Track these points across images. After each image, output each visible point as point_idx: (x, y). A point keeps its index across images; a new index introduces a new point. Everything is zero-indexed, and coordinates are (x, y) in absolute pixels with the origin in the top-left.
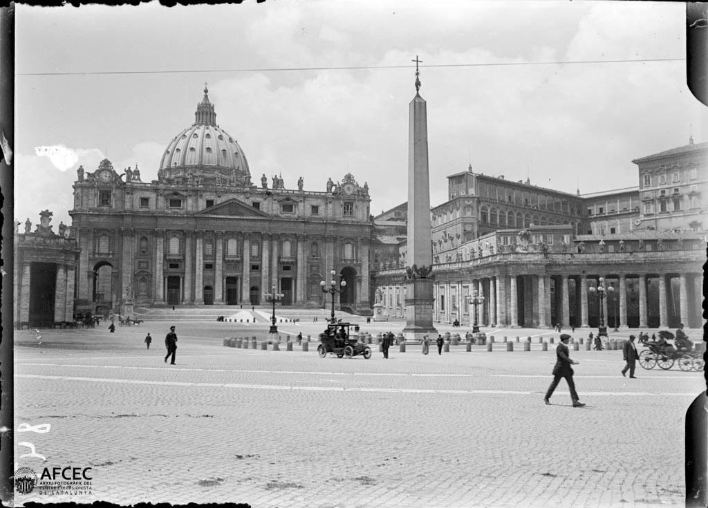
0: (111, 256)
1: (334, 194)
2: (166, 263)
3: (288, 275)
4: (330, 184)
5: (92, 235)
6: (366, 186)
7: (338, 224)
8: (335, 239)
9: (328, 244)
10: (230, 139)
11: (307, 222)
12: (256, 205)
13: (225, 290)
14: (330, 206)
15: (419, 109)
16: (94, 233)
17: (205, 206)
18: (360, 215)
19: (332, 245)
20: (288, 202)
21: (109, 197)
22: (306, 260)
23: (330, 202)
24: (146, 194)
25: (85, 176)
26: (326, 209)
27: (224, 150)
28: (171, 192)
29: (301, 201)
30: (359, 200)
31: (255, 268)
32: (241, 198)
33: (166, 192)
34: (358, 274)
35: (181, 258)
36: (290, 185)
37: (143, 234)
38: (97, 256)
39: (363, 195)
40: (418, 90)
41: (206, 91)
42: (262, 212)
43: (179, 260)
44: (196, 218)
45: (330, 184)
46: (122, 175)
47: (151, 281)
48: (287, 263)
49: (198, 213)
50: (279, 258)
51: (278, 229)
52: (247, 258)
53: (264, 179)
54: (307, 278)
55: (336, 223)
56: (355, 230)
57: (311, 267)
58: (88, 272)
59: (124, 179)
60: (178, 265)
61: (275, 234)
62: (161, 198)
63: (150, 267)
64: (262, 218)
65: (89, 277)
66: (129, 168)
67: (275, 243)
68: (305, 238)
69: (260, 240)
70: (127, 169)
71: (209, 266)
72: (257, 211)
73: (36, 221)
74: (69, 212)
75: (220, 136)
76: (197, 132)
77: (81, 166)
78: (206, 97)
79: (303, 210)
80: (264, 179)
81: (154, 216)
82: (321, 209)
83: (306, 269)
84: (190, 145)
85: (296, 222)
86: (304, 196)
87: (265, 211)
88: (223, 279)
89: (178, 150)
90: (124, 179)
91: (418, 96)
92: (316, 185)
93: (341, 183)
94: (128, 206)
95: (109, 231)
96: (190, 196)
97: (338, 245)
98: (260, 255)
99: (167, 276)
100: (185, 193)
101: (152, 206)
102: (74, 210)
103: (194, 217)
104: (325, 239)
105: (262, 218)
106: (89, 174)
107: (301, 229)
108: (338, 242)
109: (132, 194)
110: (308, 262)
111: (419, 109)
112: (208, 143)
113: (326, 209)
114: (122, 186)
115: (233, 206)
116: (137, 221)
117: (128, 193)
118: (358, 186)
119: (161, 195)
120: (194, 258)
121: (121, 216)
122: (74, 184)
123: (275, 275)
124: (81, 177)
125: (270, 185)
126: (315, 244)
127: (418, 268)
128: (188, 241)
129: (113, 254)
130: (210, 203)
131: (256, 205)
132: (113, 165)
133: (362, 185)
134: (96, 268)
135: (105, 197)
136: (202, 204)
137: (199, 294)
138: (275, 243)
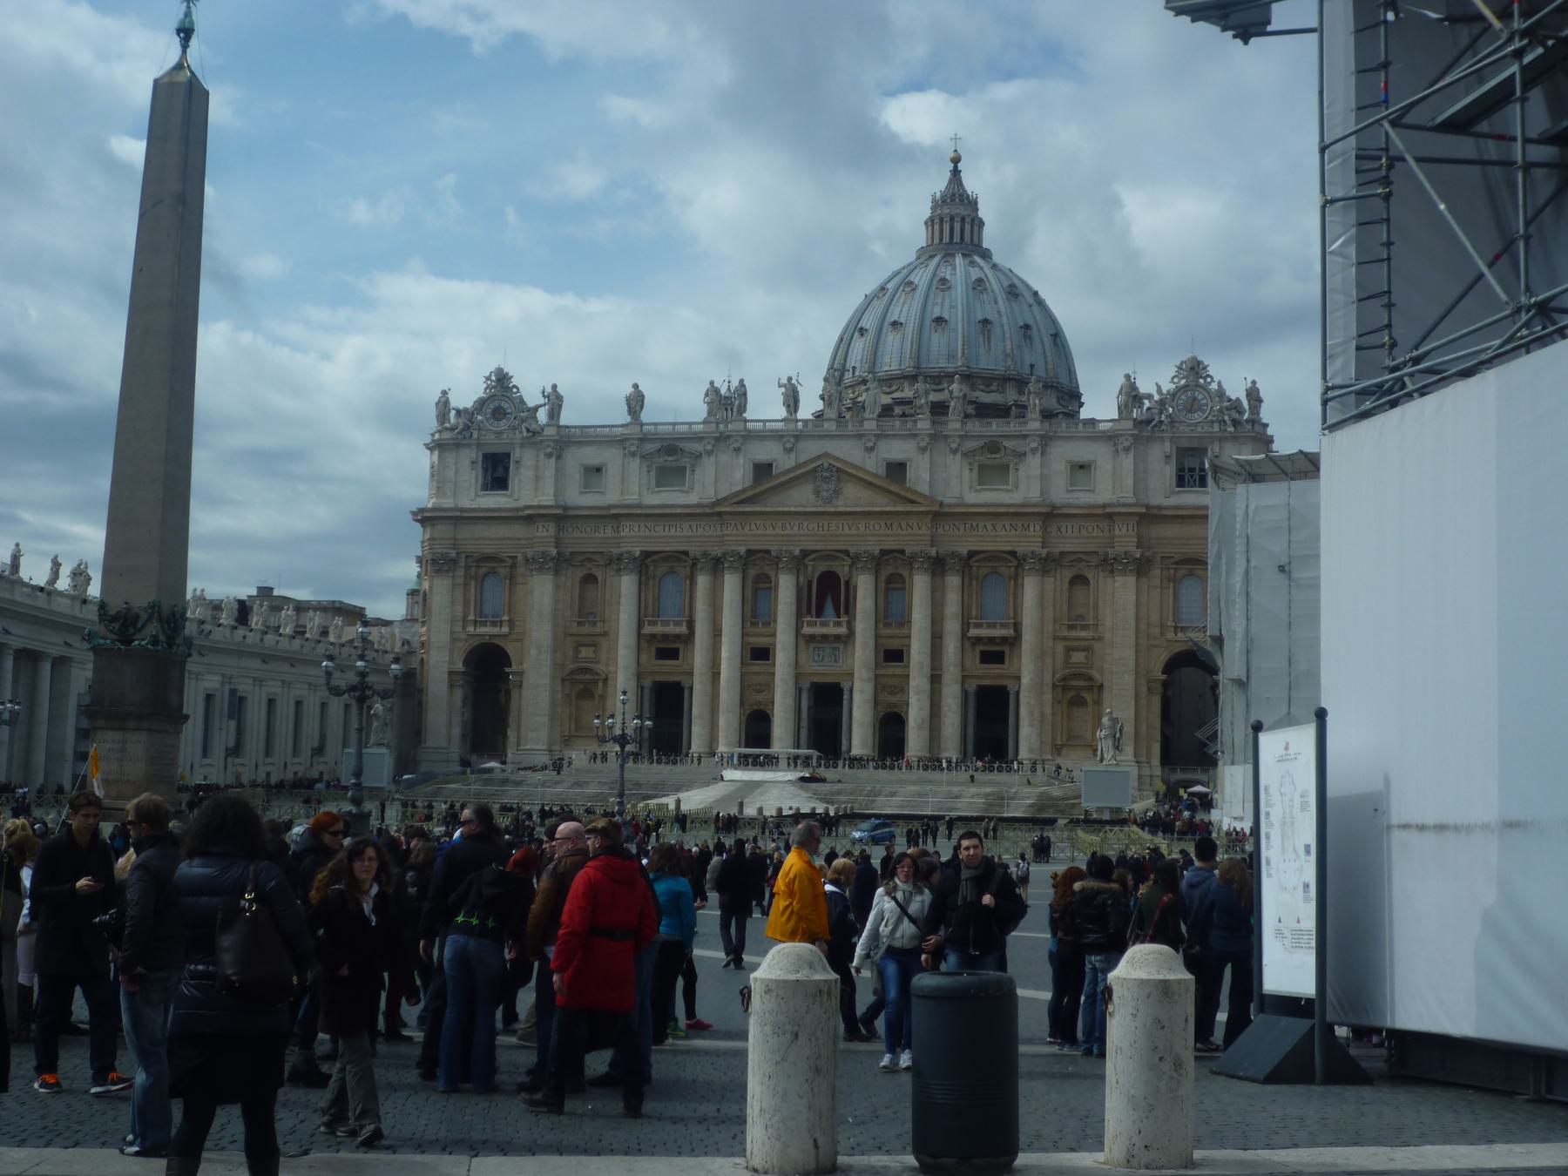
0: (505, 629)
1: (1138, 423)
2: (644, 644)
3: (991, 675)
5: (461, 572)
6: (1254, 395)
7: (1149, 516)
8: (1141, 567)
9: (1120, 580)
10: (1012, 286)
11: (1051, 516)
12: (897, 469)
13: (804, 723)
14: (1127, 462)
16: (467, 567)
17: (749, 482)
19: (1131, 580)
21: (507, 470)
22: (1049, 628)
23: (1127, 450)
24: (592, 456)
27: (986, 322)
28: (657, 445)
29: (1034, 451)
30: (1221, 439)
31: (895, 655)
33: (649, 447)
35: (683, 629)
37: (589, 565)
38: (471, 629)
40: (185, 46)
41: (956, 161)
42: (915, 492)
43: (678, 637)
44: (720, 514)
46: (536, 408)
47: (603, 697)
48: (992, 640)
49: (719, 502)
50: (965, 626)
51: (963, 541)
54: (1054, 686)
55: (1142, 516)
57: (1069, 650)
58: (451, 673)
59: (542, 416)
60: (677, 650)
61: (954, 555)
62: (635, 464)
64: (909, 508)
65: (451, 686)
66: (554, 387)
67: (953, 581)
68: (1048, 564)
70: (549, 390)
72: (894, 488)
74: (414, 514)
75: (980, 281)
76: (946, 272)
77: (444, 393)
78: (956, 173)
81: (615, 517)
83: (1049, 660)
84: (894, 316)
85: (1017, 515)
87: (924, 489)
88: (799, 690)
89: (862, 331)
90: (542, 416)
93: (1167, 387)
94: (546, 498)
95: (500, 560)
96: (709, 453)
97: (1157, 582)
98: (905, 622)
99: (647, 683)
100: (697, 447)
101: (611, 495)
102: (421, 510)
103: (711, 513)
104: (1109, 564)
105: (909, 508)
106: (459, 412)
107: (1028, 540)
108: (1156, 572)
109: (559, 457)
110: (1055, 638)
114: (534, 436)
117: (549, 456)
118: (1221, 393)
119: (633, 454)
120: (716, 633)
121: (530, 517)
122: (429, 440)
127: (112, 612)
128: (703, 581)
129: (511, 623)
130: (762, 470)
131: (897, 469)
132: (515, 381)
133: (1236, 391)
135: (496, 472)
136: (738, 476)
138: (953, 581)
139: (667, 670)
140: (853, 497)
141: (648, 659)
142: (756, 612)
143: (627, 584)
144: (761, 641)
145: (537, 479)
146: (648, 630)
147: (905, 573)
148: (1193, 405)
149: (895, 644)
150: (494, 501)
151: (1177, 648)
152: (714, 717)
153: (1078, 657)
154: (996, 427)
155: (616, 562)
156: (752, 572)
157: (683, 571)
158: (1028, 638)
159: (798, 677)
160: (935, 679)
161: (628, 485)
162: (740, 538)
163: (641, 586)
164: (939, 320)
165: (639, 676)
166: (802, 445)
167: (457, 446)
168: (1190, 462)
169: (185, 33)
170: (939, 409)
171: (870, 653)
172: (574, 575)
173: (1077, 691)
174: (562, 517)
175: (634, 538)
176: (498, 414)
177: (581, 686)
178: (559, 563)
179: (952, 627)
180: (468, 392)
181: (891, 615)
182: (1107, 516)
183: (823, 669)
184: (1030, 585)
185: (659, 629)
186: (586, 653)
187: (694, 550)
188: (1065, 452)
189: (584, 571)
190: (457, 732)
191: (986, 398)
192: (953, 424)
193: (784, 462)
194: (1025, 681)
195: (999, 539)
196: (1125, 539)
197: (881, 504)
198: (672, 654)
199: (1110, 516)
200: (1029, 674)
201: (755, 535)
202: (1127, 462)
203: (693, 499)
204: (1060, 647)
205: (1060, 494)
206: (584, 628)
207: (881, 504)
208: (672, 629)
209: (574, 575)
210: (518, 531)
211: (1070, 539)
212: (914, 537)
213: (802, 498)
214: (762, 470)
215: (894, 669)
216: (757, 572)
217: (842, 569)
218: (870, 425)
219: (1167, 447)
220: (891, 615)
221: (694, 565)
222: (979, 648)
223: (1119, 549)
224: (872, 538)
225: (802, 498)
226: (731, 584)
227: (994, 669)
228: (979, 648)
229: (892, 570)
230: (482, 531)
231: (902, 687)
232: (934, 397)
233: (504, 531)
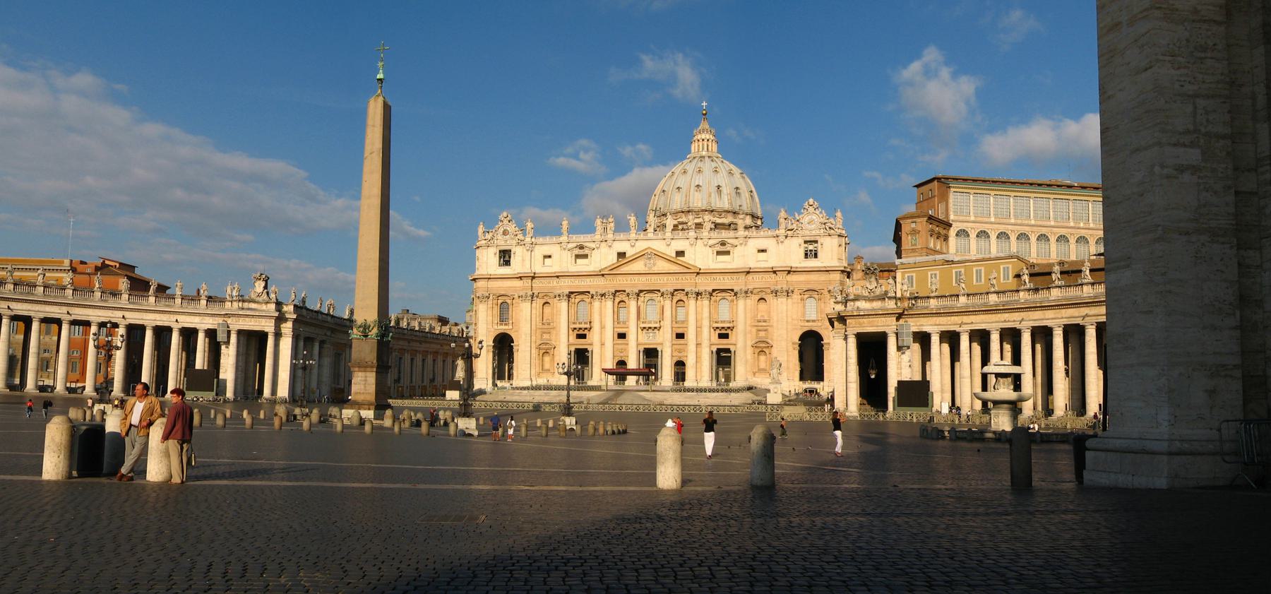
8: (788, 293)
22: (749, 322)
32: (659, 246)
34: (825, 341)
52: (667, 324)
56: (823, 277)
63: (553, 337)
69: (685, 298)
98: (685, 321)
99: (573, 349)
100: (593, 245)
101: (553, 267)
107: (738, 283)
108: (796, 296)
112: (698, 180)
116: (537, 283)
120: (602, 327)
123: (705, 343)
128: (596, 304)
130: (621, 255)
131: (680, 254)
136: (613, 259)
139: (581, 344)
140: (662, 266)
141: (573, 338)
143: (564, 305)
146: (573, 326)
147: (685, 298)
149: (680, 331)
150: (505, 271)
151: (806, 329)
153: (762, 334)
154: (724, 234)
156: (617, 300)
157: (587, 298)
158: (740, 327)
159: (638, 345)
160: (698, 345)
164: (698, 186)
166: (638, 244)
168: (811, 247)
170: (699, 226)
172: (538, 303)
173: (762, 347)
175: (566, 285)
177: (545, 350)
179: (706, 323)
183: (649, 340)
185: (577, 326)
186: (546, 336)
187: (592, 292)
190: (490, 371)
191: (719, 221)
192: (705, 233)
193: (630, 252)
194: (740, 345)
195: (726, 282)
196: (782, 281)
198: (584, 336)
199: (775, 272)
200: (741, 345)
201: (620, 282)
204: (754, 330)
205: (752, 264)
206: (546, 326)
208: (583, 326)
209: (538, 303)
211: (755, 282)
212: (688, 283)
213: (638, 266)
214: (621, 255)
215: (681, 341)
218: (668, 235)
219: (801, 241)
222: (718, 331)
223: (778, 288)
224: (668, 284)
225: (638, 266)
226: (609, 304)
227: (724, 341)
228: (718, 331)
232: (697, 221)
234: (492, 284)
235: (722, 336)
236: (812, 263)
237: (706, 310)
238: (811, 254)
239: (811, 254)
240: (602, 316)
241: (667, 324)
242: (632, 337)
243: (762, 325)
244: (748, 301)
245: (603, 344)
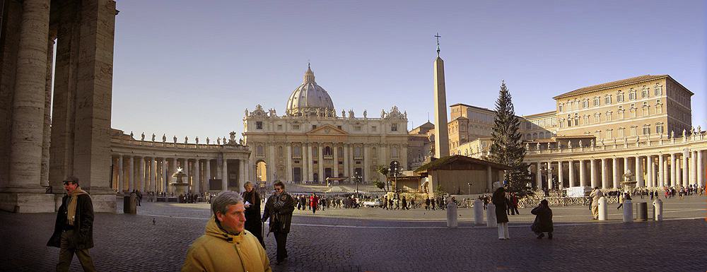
4: (384, 113)
6: (405, 113)
8: (386, 146)
9: (382, 148)
15: (440, 63)
18: (400, 132)
20: (358, 124)
21: (261, 124)
25: (249, 115)
26: (381, 129)
31: (340, 163)
36: (359, 115)
39: (403, 119)
45: (384, 113)
50: (354, 157)
52: (336, 157)
53: (344, 112)
56: (399, 139)
59: (269, 115)
67: (351, 148)
71: (315, 162)
73: (228, 138)
79: (366, 130)
80: (344, 112)
82: (378, 127)
86: (366, 121)
90: (269, 115)
91: (439, 58)
92: (374, 114)
94: (271, 130)
103: (306, 135)
104: (380, 145)
108: (389, 147)
111: (440, 63)
113: (381, 129)
115: (327, 127)
124: (247, 114)
125: (347, 115)
126: (374, 148)
128: (304, 148)
130: (314, 127)
131: (340, 127)
133: (403, 113)
134: (257, 163)
135: (259, 125)
136: (310, 127)
137: (311, 176)
138: (351, 148)
139: (297, 165)
140: (332, 132)
142: (315, 154)
143: (289, 148)
144: (316, 160)
145: (268, 127)
148: (395, 115)
149: (341, 161)
150: (259, 131)
152: (308, 174)
155: (286, 144)
160: (349, 167)
161: (288, 129)
162: (311, 140)
163: (292, 148)
165: (292, 166)
167: (251, 120)
169: (438, 51)
171: (337, 163)
174: (275, 135)
175: (290, 139)
176: (259, 114)
178: (275, 144)
180: (252, 109)
181: (341, 155)
182: (379, 136)
184: (366, 149)
188: (370, 125)
189: (280, 147)
194: (366, 167)
197: (338, 133)
200: (366, 166)
202: (383, 126)
203: (301, 132)
207: (338, 133)
210: (265, 137)
211: (373, 141)
212: (344, 140)
213: (323, 132)
214: (314, 127)
216: (315, 146)
217: (331, 146)
220: (341, 155)
221: (302, 145)
224: (337, 141)
225: (323, 132)
226: (310, 148)
229: (341, 146)
230: (257, 137)
231: (343, 168)
233: (261, 137)
234: (254, 137)
235: (357, 163)
236: (394, 133)
237: (351, 151)
238: (394, 129)
239: (394, 129)
240: (308, 155)
241: (336, 157)
242: (321, 163)
243: (374, 156)
244: (369, 149)
245: (308, 166)
